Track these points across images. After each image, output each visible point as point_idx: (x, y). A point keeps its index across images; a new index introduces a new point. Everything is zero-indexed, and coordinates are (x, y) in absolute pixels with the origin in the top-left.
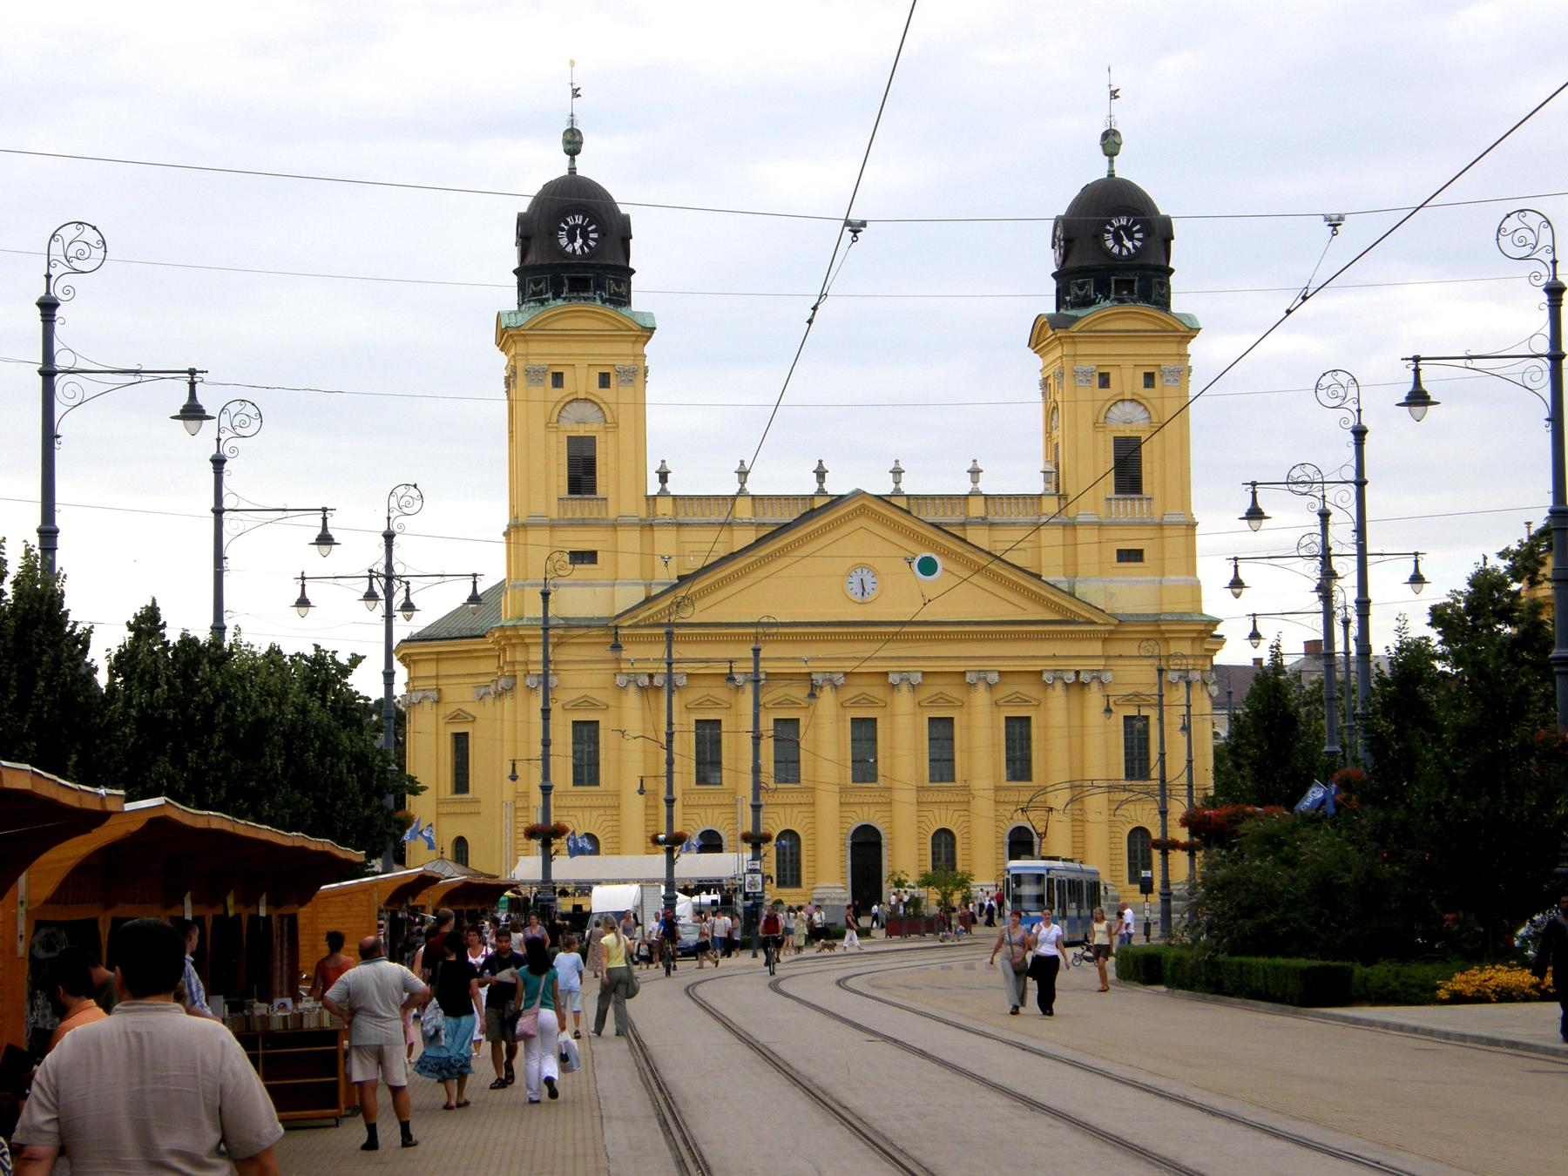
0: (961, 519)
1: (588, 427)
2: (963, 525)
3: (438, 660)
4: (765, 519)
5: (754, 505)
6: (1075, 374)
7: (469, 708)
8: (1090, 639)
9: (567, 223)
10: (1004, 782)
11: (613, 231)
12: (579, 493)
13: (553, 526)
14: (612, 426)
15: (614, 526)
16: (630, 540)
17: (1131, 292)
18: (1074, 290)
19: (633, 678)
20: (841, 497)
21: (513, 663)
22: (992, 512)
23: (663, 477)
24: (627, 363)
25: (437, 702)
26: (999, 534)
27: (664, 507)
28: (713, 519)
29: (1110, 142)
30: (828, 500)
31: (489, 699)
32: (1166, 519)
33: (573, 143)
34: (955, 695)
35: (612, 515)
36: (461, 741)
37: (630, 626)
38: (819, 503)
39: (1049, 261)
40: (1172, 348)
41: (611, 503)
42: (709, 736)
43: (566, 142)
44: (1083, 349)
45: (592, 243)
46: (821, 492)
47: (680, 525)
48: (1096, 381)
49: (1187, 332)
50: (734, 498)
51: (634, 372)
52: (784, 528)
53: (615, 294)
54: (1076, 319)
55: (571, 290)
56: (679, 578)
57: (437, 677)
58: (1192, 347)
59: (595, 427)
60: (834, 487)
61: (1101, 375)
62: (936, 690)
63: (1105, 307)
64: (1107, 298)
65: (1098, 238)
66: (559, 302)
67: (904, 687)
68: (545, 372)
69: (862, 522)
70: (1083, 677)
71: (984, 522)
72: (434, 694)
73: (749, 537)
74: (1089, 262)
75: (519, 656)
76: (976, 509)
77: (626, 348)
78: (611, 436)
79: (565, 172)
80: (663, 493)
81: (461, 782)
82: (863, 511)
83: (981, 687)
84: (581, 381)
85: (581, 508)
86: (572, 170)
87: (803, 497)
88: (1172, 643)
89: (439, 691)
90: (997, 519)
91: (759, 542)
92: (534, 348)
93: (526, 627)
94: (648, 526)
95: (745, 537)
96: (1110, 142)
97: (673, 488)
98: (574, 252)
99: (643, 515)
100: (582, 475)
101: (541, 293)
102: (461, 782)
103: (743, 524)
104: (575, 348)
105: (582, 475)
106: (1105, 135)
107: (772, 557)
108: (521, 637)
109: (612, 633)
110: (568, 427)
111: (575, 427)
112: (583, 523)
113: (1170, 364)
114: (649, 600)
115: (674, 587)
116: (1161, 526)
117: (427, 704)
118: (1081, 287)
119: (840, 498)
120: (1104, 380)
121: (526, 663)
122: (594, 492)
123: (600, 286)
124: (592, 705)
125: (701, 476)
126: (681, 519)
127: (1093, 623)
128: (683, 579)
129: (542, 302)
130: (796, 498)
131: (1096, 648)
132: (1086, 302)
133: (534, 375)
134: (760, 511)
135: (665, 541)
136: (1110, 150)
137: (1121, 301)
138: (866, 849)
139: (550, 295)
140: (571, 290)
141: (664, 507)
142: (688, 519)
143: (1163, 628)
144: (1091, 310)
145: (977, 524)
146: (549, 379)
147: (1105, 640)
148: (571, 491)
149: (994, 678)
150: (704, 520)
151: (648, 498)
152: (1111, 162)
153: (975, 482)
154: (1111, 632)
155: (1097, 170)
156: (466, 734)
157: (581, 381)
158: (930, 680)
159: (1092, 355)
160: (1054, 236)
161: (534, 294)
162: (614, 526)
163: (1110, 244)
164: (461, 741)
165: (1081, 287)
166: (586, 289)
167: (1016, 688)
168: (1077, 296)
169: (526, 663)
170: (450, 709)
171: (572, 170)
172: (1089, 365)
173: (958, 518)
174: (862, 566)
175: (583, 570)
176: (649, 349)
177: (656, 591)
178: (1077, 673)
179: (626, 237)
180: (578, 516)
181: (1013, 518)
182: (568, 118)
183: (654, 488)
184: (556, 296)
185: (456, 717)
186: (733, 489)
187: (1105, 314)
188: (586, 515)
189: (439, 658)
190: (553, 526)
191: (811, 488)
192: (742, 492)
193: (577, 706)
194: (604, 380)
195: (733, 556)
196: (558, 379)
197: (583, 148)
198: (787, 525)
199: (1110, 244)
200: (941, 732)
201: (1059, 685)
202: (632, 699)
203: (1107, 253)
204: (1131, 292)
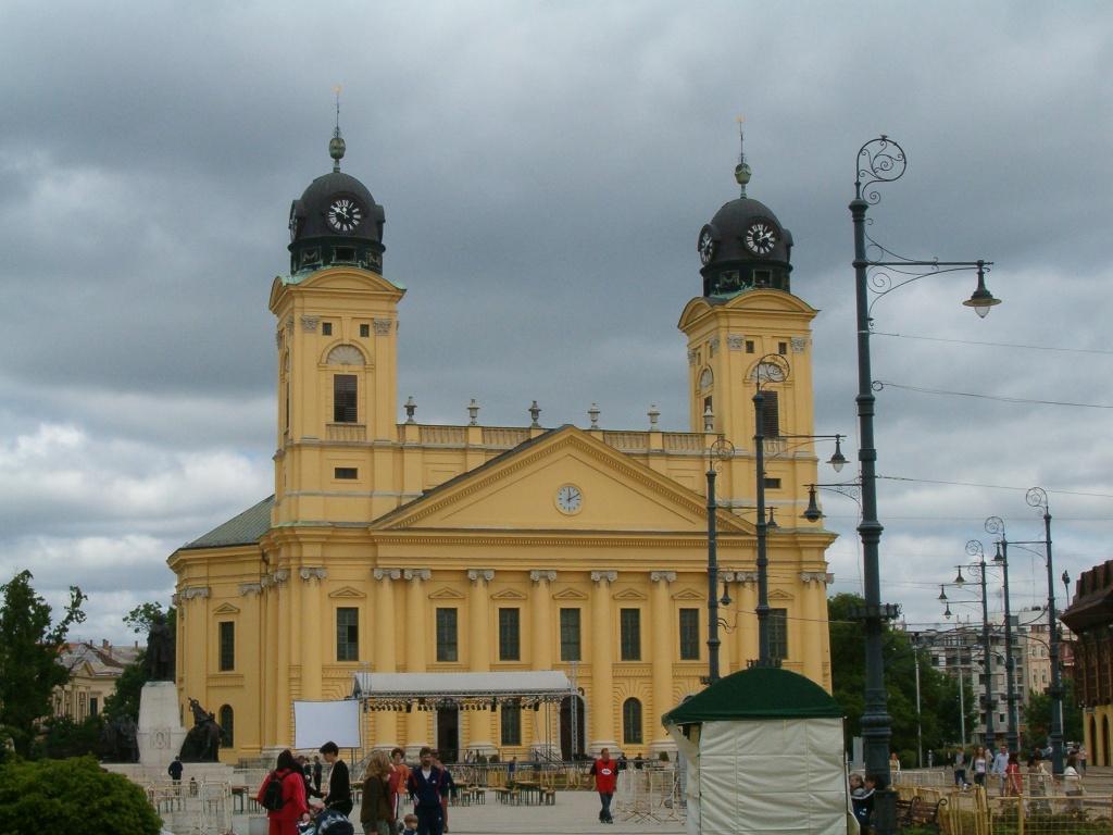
0: (645, 451)
1: (351, 368)
2: (646, 455)
3: (208, 565)
4: (494, 446)
5: (483, 435)
6: (729, 341)
7: (235, 603)
8: (744, 547)
10: (679, 661)
11: (374, 218)
13: (322, 446)
14: (369, 367)
15: (371, 448)
16: (384, 460)
19: (387, 573)
20: (551, 430)
21: (288, 559)
22: (667, 446)
23: (411, 410)
24: (384, 317)
25: (208, 598)
26: (675, 464)
27: (412, 435)
28: (451, 444)
29: (742, 174)
30: (541, 432)
31: (252, 596)
32: (798, 455)
33: (337, 154)
34: (640, 590)
35: (370, 440)
36: (227, 630)
37: (386, 530)
38: (534, 434)
39: (696, 262)
40: (799, 325)
41: (369, 428)
42: (447, 623)
43: (332, 148)
44: (734, 322)
45: (356, 223)
46: (536, 427)
47: (424, 449)
48: (744, 347)
49: (808, 314)
50: (466, 428)
52: (507, 454)
53: (373, 264)
54: (728, 301)
55: (339, 258)
56: (424, 491)
57: (208, 578)
58: (813, 324)
59: (357, 368)
60: (546, 422)
61: (747, 343)
62: (625, 587)
63: (748, 292)
64: (749, 284)
65: (741, 240)
66: (329, 267)
67: (603, 583)
68: (317, 322)
70: (739, 578)
71: (662, 454)
72: (205, 592)
74: (736, 258)
75: (294, 552)
76: (656, 443)
77: (383, 306)
78: (369, 376)
79: (332, 171)
80: (410, 424)
81: (227, 661)
82: (571, 441)
83: (662, 584)
84: (347, 330)
85: (345, 433)
86: (336, 170)
87: (522, 430)
88: (804, 552)
89: (210, 589)
90: (672, 452)
91: (487, 465)
92: (309, 302)
93: (300, 528)
94: (400, 449)
95: (476, 461)
96: (742, 174)
97: (418, 419)
99: (394, 439)
100: (346, 407)
101: (314, 260)
102: (227, 661)
103: (475, 449)
104: (344, 304)
105: (346, 407)
106: (739, 168)
107: (500, 476)
108: (296, 537)
109: (368, 535)
110: (335, 368)
111: (341, 367)
112: (346, 446)
113: (797, 336)
114: (400, 509)
115: (420, 499)
116: (793, 461)
117: (199, 600)
118: (729, 277)
119: (550, 432)
120: (750, 347)
121: (300, 558)
122: (355, 421)
123: (362, 257)
124: (355, 595)
126: (424, 444)
127: (748, 534)
128: (427, 493)
129: (315, 268)
130: (516, 430)
132: (733, 288)
133: (308, 324)
134: (487, 440)
135: (412, 460)
136: (743, 178)
137: (760, 287)
138: (572, 712)
139: (321, 262)
140: (339, 258)
141: (412, 435)
142: (431, 444)
143: (799, 539)
144: (736, 294)
145: (658, 455)
146: (320, 327)
148: (336, 419)
149: (673, 577)
150: (445, 445)
152: (743, 188)
155: (732, 192)
156: (231, 624)
157: (347, 330)
158: (624, 579)
159: (739, 328)
160: (701, 240)
161: (305, 263)
162: (371, 448)
163: (751, 244)
164: (227, 630)
166: (348, 258)
167: (689, 586)
168: (726, 283)
169: (300, 558)
170: (219, 603)
171: (336, 170)
172: (738, 334)
173: (641, 449)
174: (569, 486)
175: (345, 485)
177: (405, 502)
178: (736, 574)
179: (380, 222)
180: (342, 439)
181: (683, 452)
182: (333, 128)
183: (403, 419)
184: (326, 263)
185: (224, 610)
186: (466, 422)
187: (747, 297)
188: (348, 440)
189: (210, 562)
190: (322, 446)
191: (528, 423)
192: (473, 425)
193: (340, 595)
194: (364, 330)
195: (467, 475)
196: (327, 329)
198: (510, 451)
199: (751, 244)
200: (630, 620)
202: (387, 590)
203: (748, 251)
204: (768, 282)
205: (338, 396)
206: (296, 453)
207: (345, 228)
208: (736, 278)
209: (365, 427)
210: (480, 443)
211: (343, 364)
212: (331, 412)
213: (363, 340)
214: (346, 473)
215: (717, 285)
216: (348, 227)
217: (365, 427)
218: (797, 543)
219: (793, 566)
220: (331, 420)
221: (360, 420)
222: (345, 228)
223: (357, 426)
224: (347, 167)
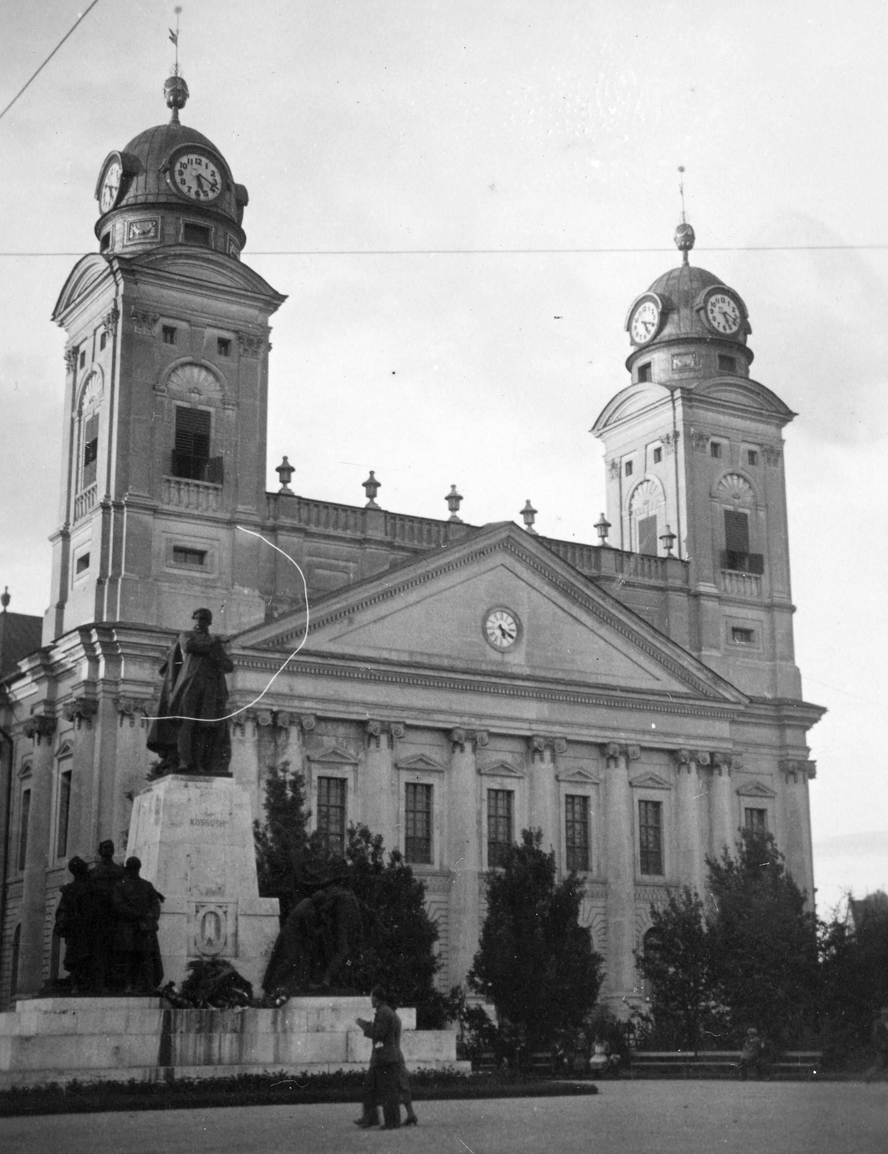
23: (286, 471)
40: (770, 430)
51: (260, 342)
60: (470, 515)
68: (155, 321)
69: (501, 558)
86: (175, 120)
97: (299, 486)
98: (179, 209)
125: (330, 480)
131: (722, 728)
143: (785, 713)
147: (733, 722)
151: (270, 495)
153: (603, 537)
154: (742, 714)
155: (675, 260)
167: (649, 768)
171: (175, 120)
176: (273, 320)
183: (273, 485)
197: (188, 102)
201: (693, 766)
205: (180, 435)
210: (383, 534)
211: (191, 391)
218: (779, 718)
219: (774, 752)
224: (187, 118)
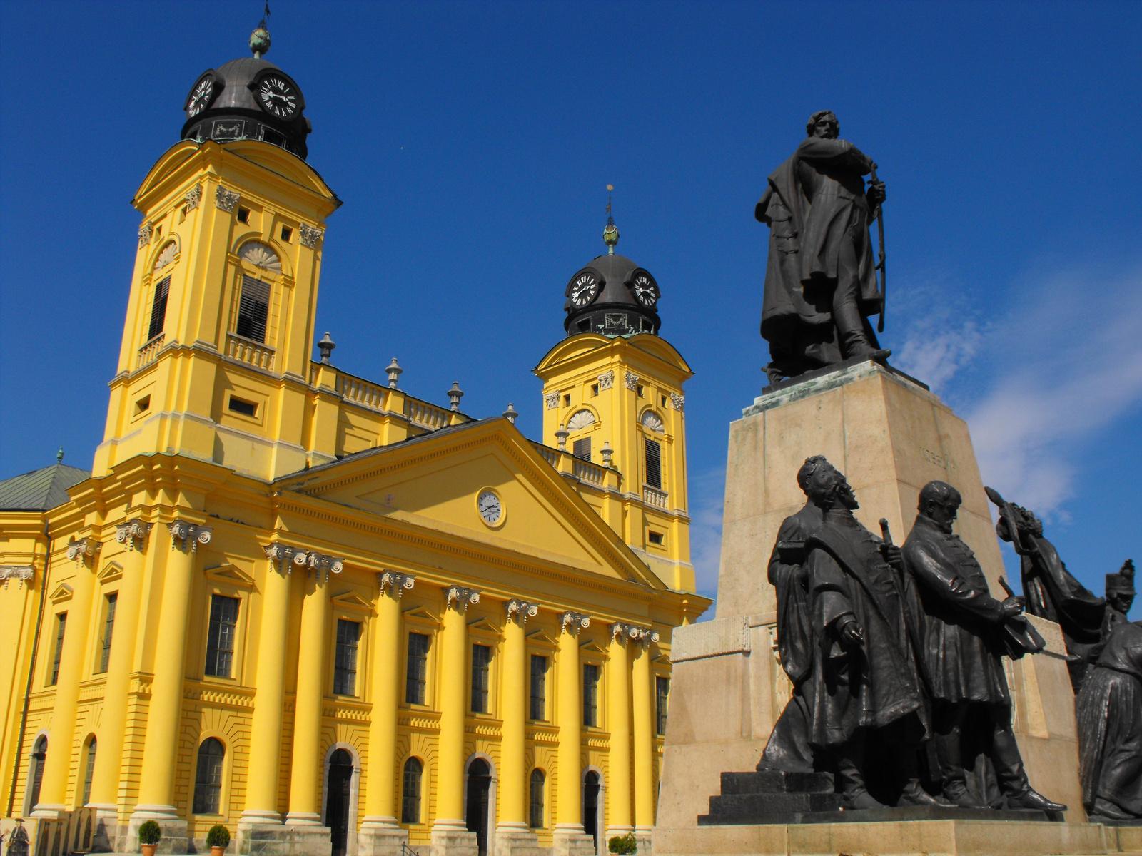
9: (270, 83)
12: (248, 336)
17: (650, 332)
18: (608, 321)
27: (325, 379)
38: (454, 421)
45: (289, 110)
59: (271, 275)
73: (402, 434)
101: (232, 134)
105: (252, 322)
111: (254, 269)
118: (616, 318)
122: (262, 341)
148: (239, 332)
165: (616, 318)
168: (611, 323)
196: (243, 216)
198: (431, 432)
203: (636, 298)
206: (180, 360)
207: (277, 111)
208: (624, 321)
209: (272, 352)
212: (235, 320)
213: (283, 244)
214: (244, 407)
215: (601, 326)
216: (281, 111)
217: (272, 352)
220: (234, 333)
221: (268, 343)
222: (277, 111)
223: (264, 349)
